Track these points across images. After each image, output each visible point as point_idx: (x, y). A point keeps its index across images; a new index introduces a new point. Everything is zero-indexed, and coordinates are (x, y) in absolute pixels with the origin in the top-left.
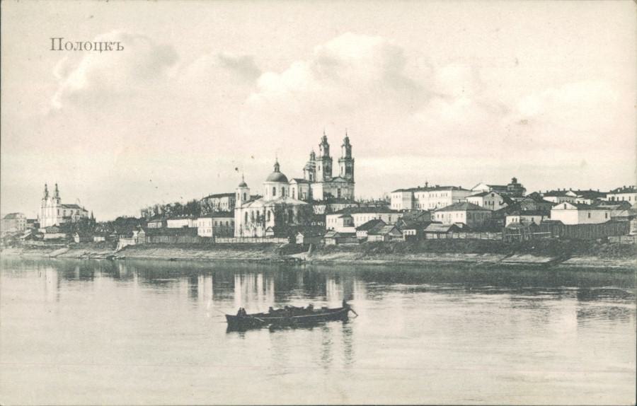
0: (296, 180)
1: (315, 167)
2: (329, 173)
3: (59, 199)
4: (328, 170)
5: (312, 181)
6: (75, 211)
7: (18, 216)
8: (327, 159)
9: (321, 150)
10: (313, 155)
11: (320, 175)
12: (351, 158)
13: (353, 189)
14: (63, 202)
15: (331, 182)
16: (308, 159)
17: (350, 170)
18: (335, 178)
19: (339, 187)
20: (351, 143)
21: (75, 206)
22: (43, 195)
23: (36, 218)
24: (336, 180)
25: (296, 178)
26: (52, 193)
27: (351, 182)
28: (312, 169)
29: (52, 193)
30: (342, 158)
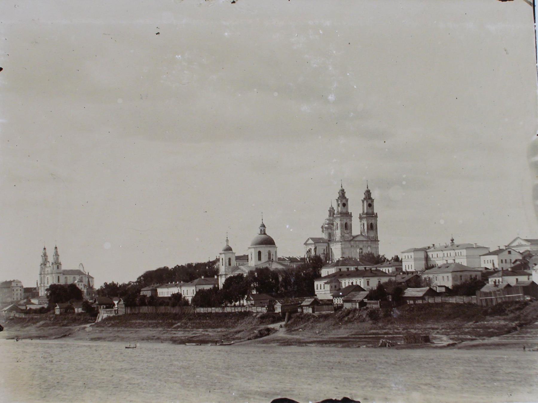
0: (313, 239)
1: (333, 224)
2: (348, 231)
3: (58, 264)
4: (347, 227)
5: (330, 240)
6: (78, 278)
7: (13, 284)
8: (347, 215)
9: (339, 205)
10: (331, 212)
11: (338, 233)
12: (373, 213)
13: (377, 248)
14: (64, 267)
15: (351, 240)
16: (327, 216)
17: (372, 227)
18: (354, 237)
19: (361, 246)
20: (373, 196)
21: (79, 273)
22: (40, 260)
23: (35, 286)
24: (356, 239)
25: (311, 237)
26: (51, 259)
27: (375, 240)
28: (329, 227)
29: (51, 259)
30: (363, 213)
